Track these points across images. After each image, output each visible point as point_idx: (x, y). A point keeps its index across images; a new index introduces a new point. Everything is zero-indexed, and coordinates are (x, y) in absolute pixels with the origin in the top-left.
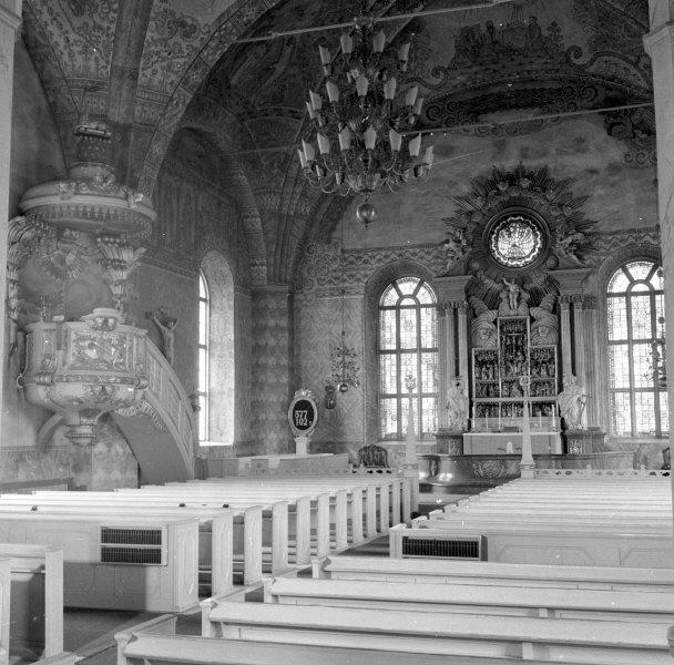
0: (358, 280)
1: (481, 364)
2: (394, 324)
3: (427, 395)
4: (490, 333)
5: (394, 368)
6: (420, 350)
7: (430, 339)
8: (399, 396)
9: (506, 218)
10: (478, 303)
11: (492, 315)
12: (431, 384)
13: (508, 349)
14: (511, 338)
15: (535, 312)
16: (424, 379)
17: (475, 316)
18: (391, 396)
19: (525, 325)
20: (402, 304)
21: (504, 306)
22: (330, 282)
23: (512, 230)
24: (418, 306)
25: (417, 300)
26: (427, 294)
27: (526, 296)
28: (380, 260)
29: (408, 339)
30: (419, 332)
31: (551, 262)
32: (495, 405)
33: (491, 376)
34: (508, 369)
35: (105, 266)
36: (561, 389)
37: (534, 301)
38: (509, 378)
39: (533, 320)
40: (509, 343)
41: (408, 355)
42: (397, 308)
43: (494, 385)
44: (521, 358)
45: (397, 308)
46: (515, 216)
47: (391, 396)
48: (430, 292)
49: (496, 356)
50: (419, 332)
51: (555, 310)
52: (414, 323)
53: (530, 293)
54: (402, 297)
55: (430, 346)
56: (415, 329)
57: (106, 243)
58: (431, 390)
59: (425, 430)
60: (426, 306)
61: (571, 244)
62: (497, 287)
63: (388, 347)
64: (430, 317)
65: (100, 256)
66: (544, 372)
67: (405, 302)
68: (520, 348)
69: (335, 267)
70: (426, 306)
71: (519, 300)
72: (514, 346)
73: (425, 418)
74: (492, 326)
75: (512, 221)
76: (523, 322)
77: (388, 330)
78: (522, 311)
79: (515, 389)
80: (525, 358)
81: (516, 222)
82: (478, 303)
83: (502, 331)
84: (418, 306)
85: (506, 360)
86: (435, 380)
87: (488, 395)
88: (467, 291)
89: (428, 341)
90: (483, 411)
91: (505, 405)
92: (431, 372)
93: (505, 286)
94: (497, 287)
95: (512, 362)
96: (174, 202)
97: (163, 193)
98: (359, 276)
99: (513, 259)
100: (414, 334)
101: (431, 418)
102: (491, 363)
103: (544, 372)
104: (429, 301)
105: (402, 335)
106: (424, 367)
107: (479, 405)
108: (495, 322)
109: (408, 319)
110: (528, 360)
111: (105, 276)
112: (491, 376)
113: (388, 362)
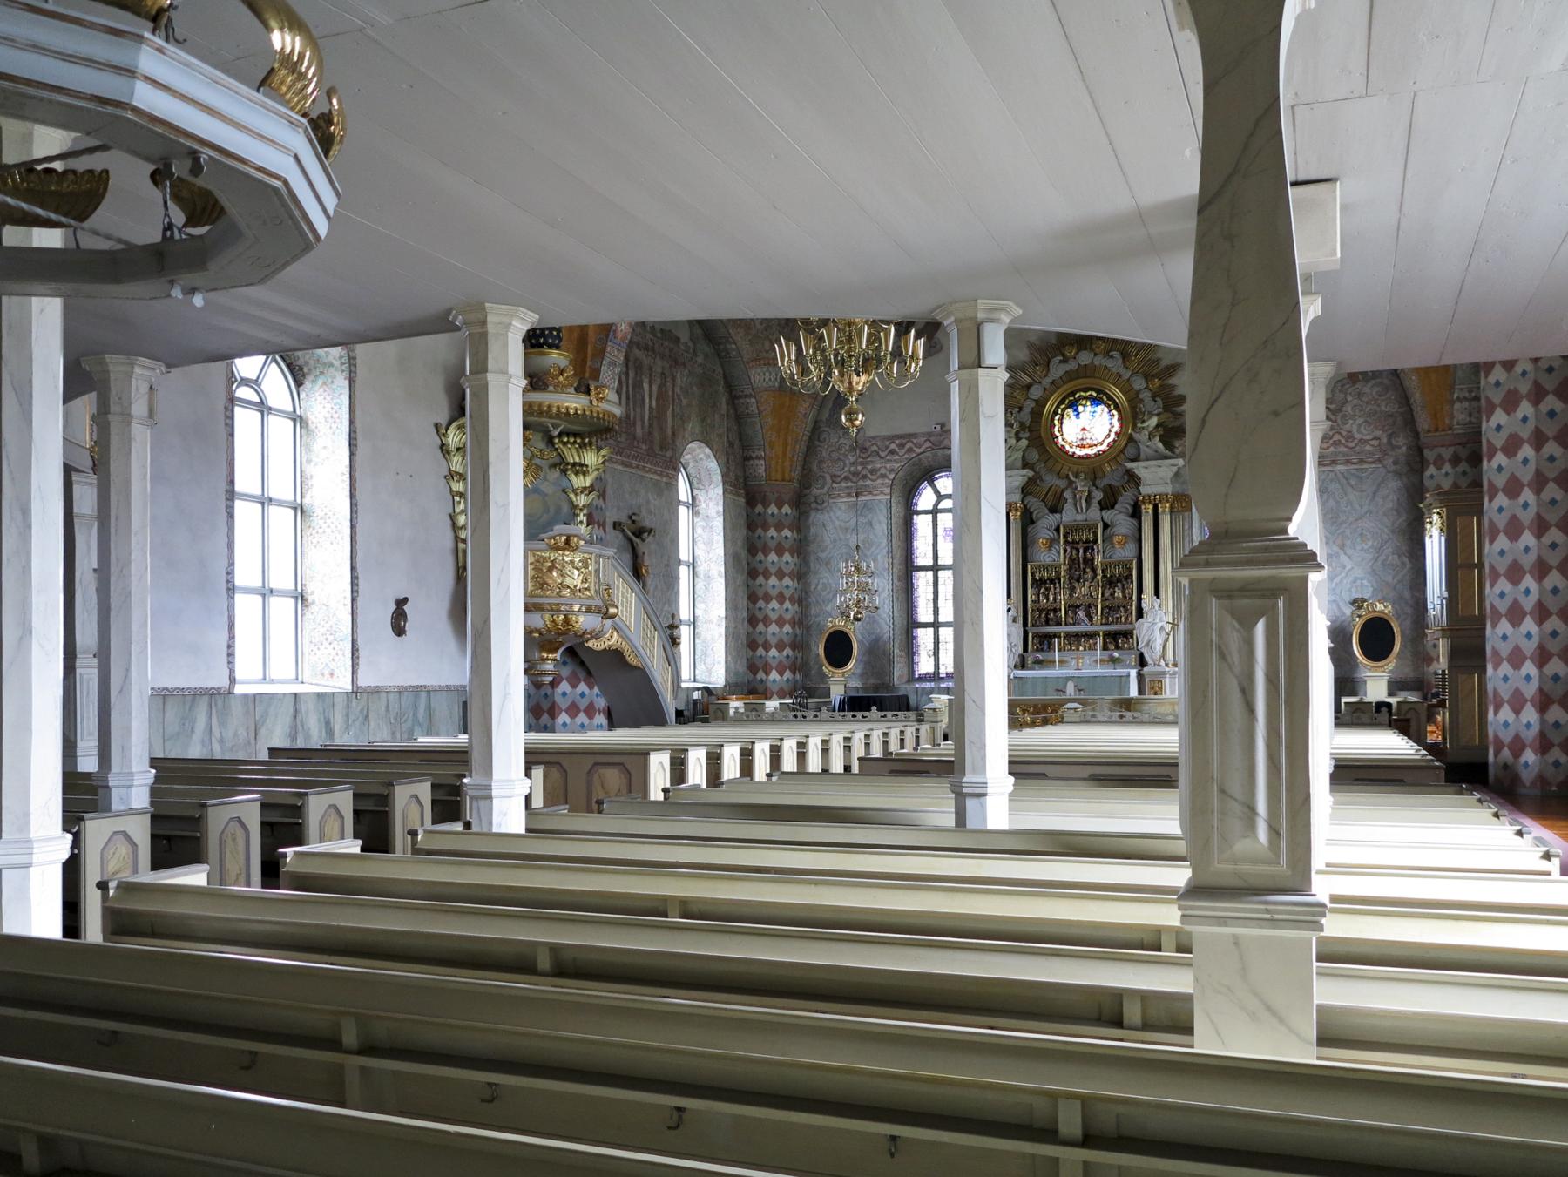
0: (883, 476)
1: (1038, 583)
4: (1052, 543)
8: (936, 625)
9: (1073, 394)
10: (1035, 504)
11: (1052, 519)
13: (1073, 562)
15: (1108, 515)
17: (1033, 522)
19: (1095, 534)
21: (1068, 507)
22: (846, 479)
23: (1081, 408)
27: (1098, 495)
28: (910, 450)
31: (1131, 451)
32: (1055, 635)
34: (1072, 589)
35: (564, 472)
36: (1140, 614)
37: (1108, 504)
39: (1106, 526)
42: (934, 512)
44: (1090, 575)
45: (934, 512)
46: (1085, 390)
49: (1058, 573)
51: (1136, 514)
53: (1104, 490)
54: (940, 497)
57: (565, 444)
61: (1157, 426)
62: (1062, 484)
65: (557, 460)
66: (1119, 594)
68: (1089, 562)
69: (852, 459)
71: (1089, 500)
72: (1080, 565)
75: (1081, 398)
76: (1092, 528)
78: (1094, 514)
79: (1081, 614)
80: (1095, 575)
81: (1086, 398)
82: (1035, 504)
83: (1066, 542)
85: (1071, 578)
87: (1047, 624)
88: (1023, 489)
90: (1041, 643)
91: (1068, 635)
93: (1071, 482)
94: (1062, 484)
96: (646, 386)
97: (631, 375)
98: (883, 471)
99: (1083, 446)
102: (1052, 582)
103: (1119, 594)
107: (1035, 636)
108: (1057, 529)
111: (565, 483)
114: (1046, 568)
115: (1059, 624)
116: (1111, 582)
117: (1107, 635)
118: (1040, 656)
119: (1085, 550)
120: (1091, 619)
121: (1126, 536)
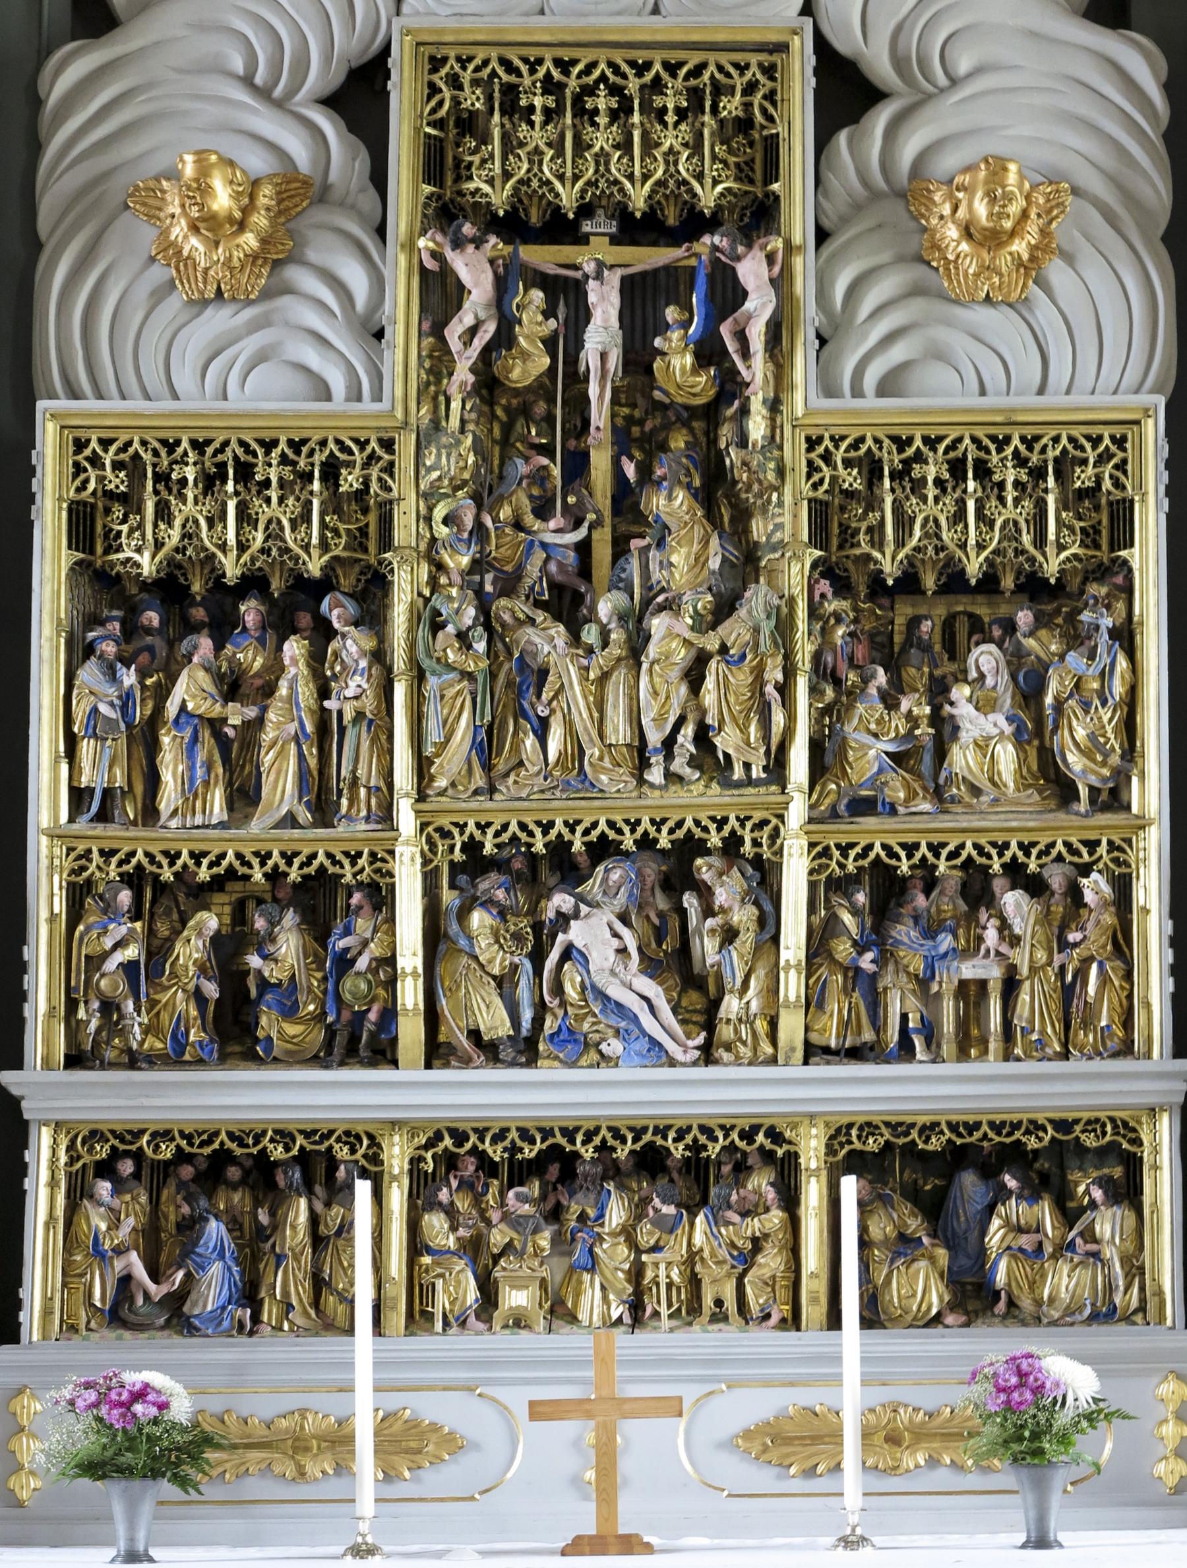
13: (520, 416)
14: (567, 294)
32: (324, 1164)
33: (281, 786)
34: (515, 690)
38: (525, 805)
40: (528, 366)
43: (318, 899)
44: (685, 558)
49: (367, 521)
66: (985, 740)
68: (690, 439)
74: (315, 141)
79: (599, 937)
80: (747, 563)
83: (445, 213)
85: (493, 580)
87: (234, 1030)
90: (165, 1244)
91: (456, 1161)
95: (567, 604)
102: (296, 604)
103: (985, 740)
107: (108, 1158)
110: (796, 575)
112: (281, 786)
114: (231, 466)
115: (363, 1042)
116: (903, 625)
117: (855, 1152)
118: (172, 1380)
119: (643, 299)
120: (697, 994)
121: (1055, 187)
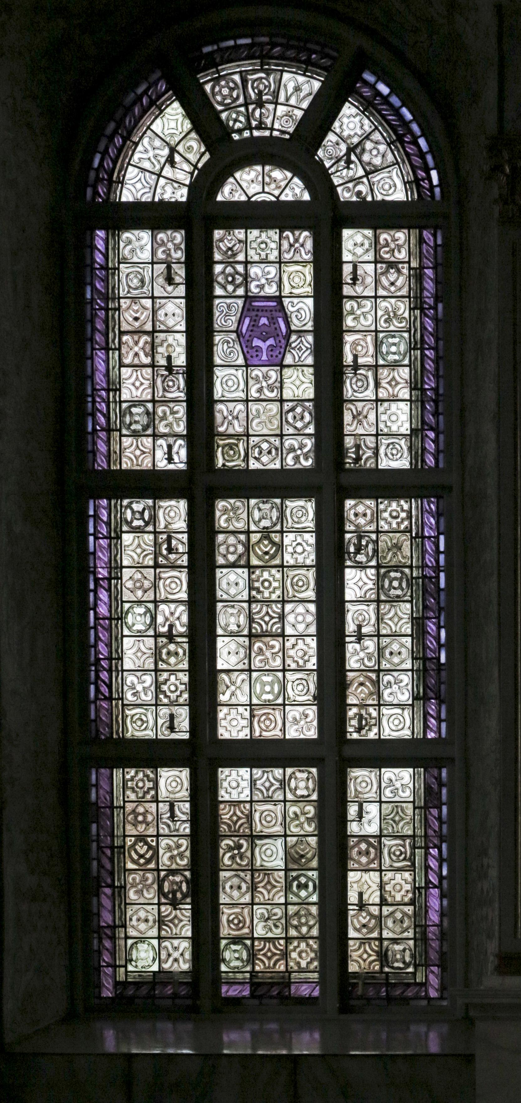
2: (174, 313)
3: (384, 754)
5: (177, 584)
6: (334, 478)
7: (400, 417)
12: (400, 689)
16: (356, 656)
18: (154, 754)
20: (228, 193)
24: (325, 217)
25: (317, 179)
26: (378, 151)
29: (263, 410)
30: (330, 371)
41: (262, 512)
45: (198, 219)
47: (154, 754)
48: (399, 137)
50: (330, 371)
52: (302, 311)
54: (299, 150)
55: (397, 460)
56: (303, 351)
58: (397, 724)
59: (360, 960)
60: (377, 216)
63: (135, 454)
64: (401, 281)
67: (247, 185)
70: (377, 216)
73: (362, 884)
77: (134, 349)
84: (325, 217)
86: (425, 667)
89: (386, 423)
92: (400, 617)
100: (301, 384)
101: (401, 884)
104: (393, 187)
105: (227, 381)
106: (357, 581)
109: (263, 280)
113: (134, 547)
